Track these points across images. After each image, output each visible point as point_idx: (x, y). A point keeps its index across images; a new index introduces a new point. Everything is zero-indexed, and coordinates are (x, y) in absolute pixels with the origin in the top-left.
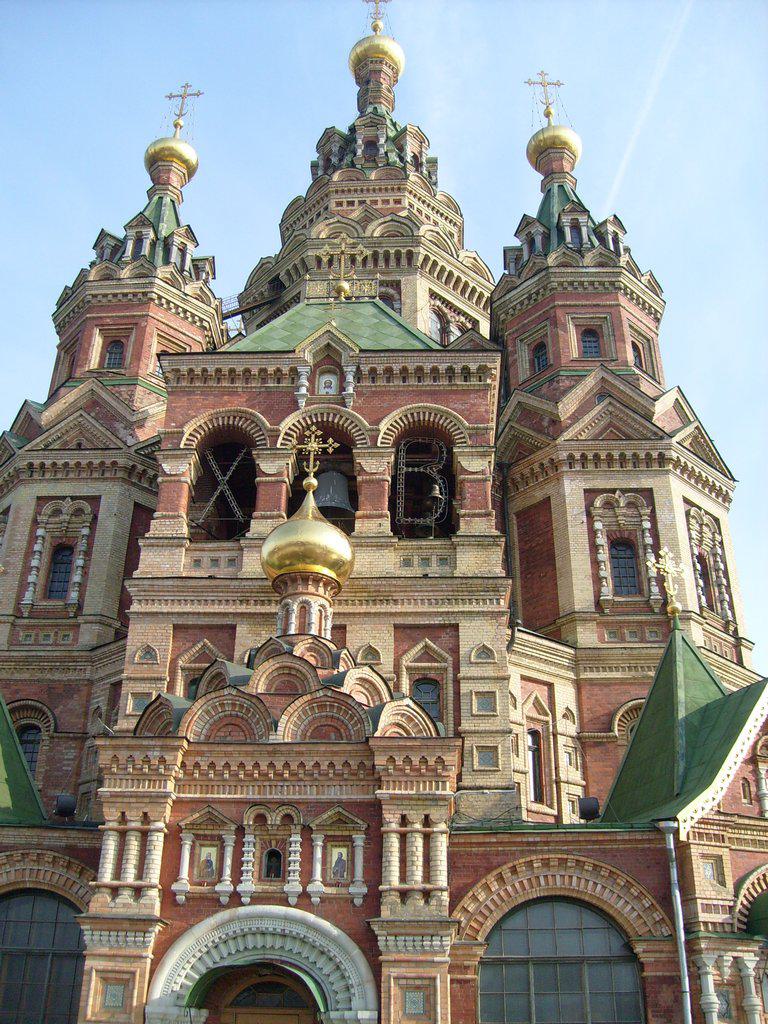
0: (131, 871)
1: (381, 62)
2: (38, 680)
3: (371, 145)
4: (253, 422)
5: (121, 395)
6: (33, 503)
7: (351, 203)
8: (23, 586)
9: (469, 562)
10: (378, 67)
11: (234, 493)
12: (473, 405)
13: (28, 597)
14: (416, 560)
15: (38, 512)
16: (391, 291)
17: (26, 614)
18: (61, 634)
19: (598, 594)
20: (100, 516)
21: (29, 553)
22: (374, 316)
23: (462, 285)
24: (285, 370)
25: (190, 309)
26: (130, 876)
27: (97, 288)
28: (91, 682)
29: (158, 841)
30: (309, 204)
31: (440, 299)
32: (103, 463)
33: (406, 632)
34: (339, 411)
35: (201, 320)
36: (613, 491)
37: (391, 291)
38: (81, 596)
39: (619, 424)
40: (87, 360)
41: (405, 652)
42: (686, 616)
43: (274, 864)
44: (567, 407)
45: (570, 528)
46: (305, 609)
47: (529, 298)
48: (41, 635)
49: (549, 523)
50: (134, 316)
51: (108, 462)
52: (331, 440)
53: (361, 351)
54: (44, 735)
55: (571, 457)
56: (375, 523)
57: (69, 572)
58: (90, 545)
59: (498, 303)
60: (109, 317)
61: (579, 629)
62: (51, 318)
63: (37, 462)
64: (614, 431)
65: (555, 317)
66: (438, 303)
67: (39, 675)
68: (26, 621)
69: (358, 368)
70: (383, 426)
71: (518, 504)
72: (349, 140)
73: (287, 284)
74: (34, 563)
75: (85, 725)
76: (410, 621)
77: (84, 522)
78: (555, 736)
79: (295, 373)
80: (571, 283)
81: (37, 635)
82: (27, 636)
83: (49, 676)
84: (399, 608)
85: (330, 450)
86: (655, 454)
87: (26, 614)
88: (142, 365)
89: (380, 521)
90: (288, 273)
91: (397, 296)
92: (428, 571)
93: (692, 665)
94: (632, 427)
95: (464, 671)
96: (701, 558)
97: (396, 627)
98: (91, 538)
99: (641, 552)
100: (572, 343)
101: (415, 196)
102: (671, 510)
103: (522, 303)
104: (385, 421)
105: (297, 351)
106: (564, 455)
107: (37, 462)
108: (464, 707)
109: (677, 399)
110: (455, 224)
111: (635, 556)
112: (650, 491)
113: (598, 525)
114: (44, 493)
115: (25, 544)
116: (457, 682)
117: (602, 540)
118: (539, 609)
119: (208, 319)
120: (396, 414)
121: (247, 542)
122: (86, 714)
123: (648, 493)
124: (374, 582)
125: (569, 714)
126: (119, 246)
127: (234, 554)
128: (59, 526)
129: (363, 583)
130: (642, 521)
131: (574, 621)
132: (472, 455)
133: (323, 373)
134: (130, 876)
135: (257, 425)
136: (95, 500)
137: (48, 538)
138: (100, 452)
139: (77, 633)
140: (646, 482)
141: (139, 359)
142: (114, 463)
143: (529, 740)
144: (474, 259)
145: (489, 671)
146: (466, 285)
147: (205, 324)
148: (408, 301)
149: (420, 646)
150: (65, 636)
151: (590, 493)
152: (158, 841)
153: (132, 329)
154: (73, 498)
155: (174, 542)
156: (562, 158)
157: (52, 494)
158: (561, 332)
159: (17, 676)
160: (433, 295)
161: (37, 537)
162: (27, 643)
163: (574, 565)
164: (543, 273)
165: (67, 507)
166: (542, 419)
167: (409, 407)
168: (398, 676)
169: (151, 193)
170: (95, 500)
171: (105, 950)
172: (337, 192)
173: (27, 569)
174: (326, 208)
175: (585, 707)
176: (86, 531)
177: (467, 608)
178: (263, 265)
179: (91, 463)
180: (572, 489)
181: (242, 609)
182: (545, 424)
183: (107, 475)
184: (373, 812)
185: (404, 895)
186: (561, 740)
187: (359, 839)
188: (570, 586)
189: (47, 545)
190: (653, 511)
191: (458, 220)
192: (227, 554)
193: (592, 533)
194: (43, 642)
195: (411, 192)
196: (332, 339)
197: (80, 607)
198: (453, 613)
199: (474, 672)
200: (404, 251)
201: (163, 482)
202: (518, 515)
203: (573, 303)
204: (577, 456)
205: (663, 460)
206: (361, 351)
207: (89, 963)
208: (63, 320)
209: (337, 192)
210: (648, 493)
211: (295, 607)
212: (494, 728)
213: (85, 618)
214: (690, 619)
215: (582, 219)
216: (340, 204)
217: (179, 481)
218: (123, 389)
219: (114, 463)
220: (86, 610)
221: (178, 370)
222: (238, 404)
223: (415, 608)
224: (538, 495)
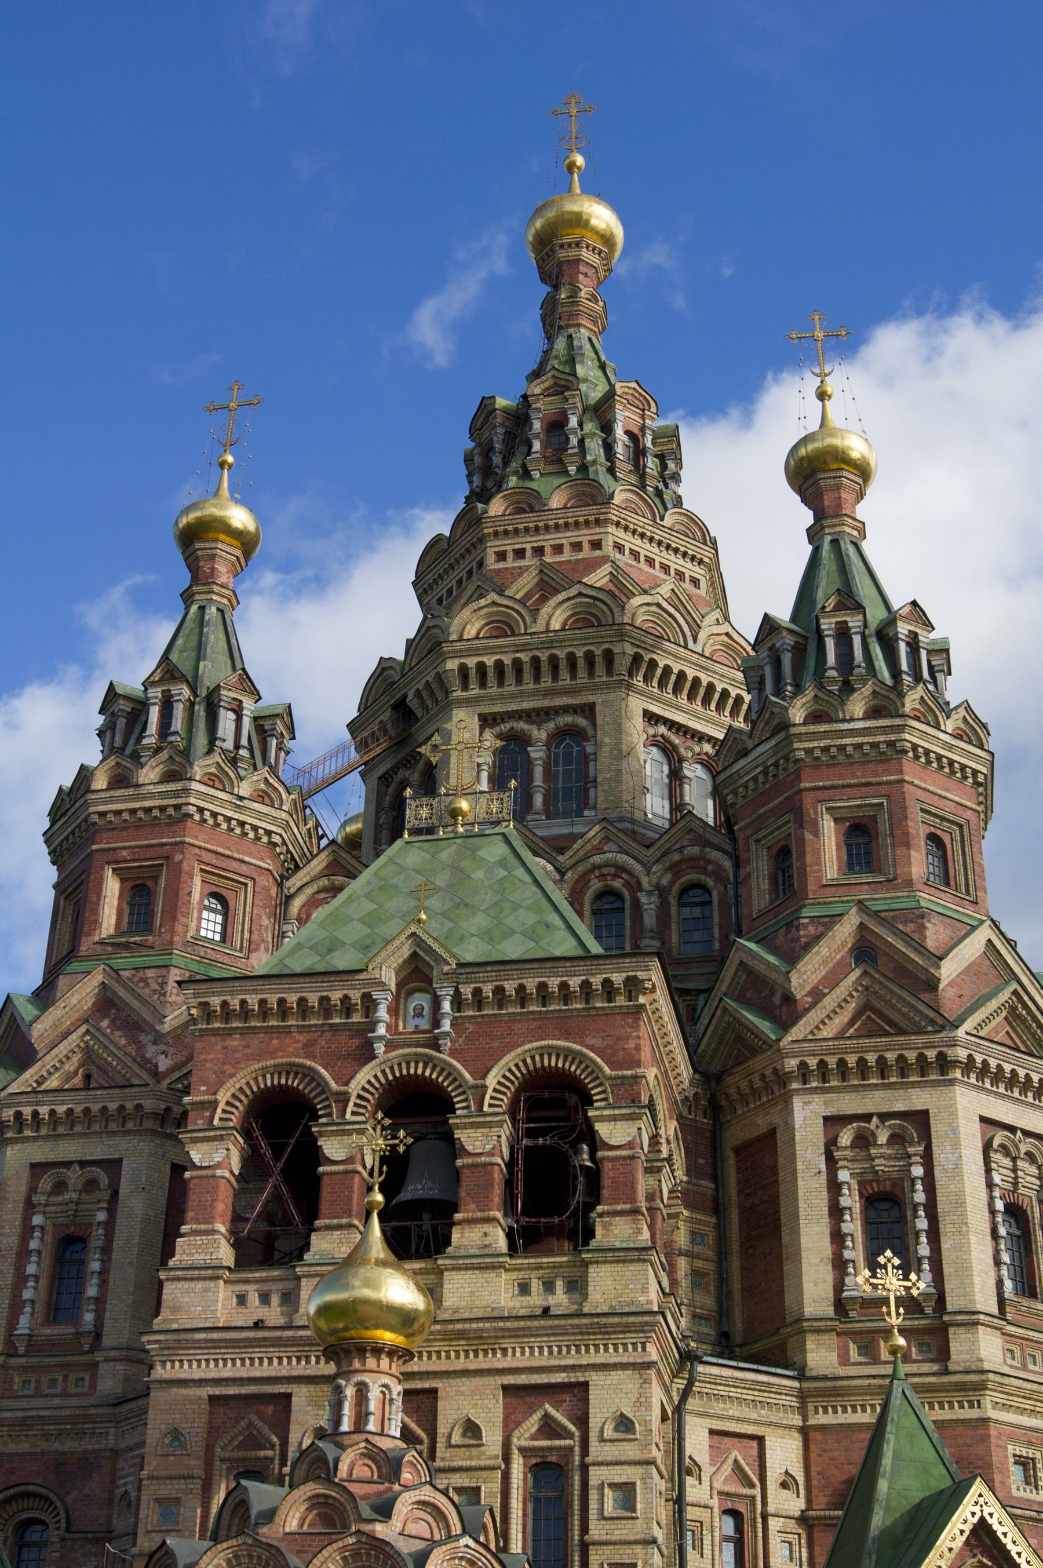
1: (578, 245)
2: (42, 1453)
3: (557, 426)
4: (313, 1079)
5: (147, 985)
6: (25, 1174)
7: (520, 554)
8: (16, 1306)
9: (605, 1286)
10: (572, 253)
12: (619, 1039)
13: (24, 1321)
14: (536, 1285)
15: (33, 1189)
16: (582, 722)
17: (22, 1350)
18: (72, 1377)
19: (839, 1287)
20: (122, 1191)
21: (23, 1254)
22: (502, 863)
23: (702, 691)
24: (356, 996)
25: (249, 820)
27: (105, 802)
28: (116, 1453)
30: (458, 550)
31: (665, 724)
32: (122, 1108)
33: (519, 1395)
34: (431, 1058)
35: (269, 833)
36: (867, 1117)
37: (582, 722)
39: (880, 1005)
40: (96, 923)
41: (518, 1424)
42: (971, 1321)
44: (804, 977)
45: (800, 1183)
46: (362, 1390)
47: (765, 772)
48: (45, 1379)
49: (774, 1169)
50: (163, 845)
51: (130, 1106)
52: (402, 1134)
53: (460, 965)
54: (54, 1535)
55: (803, 1065)
56: (480, 1233)
57: (81, 1279)
58: (109, 1237)
60: (124, 848)
61: (810, 1345)
62: (42, 839)
64: (873, 1018)
65: (801, 808)
66: (662, 729)
67: (43, 1445)
68: (21, 1361)
69: (457, 989)
70: (491, 1081)
71: (737, 1133)
72: (520, 417)
73: (419, 713)
74: (31, 1269)
75: (109, 1518)
76: (523, 1379)
77: (99, 1202)
78: (765, 1517)
79: (369, 1004)
80: (826, 749)
81: (38, 1381)
82: (25, 1382)
83: (57, 1446)
84: (508, 1362)
85: (401, 1149)
86: (931, 1054)
87: (22, 1350)
88: (179, 929)
89: (487, 1228)
90: (418, 694)
91: (590, 731)
92: (552, 1300)
93: (911, 1437)
94: (899, 1011)
95: (596, 1450)
96: (1015, 1212)
97: (506, 1389)
98: (109, 1226)
99: (909, 1213)
100: (827, 847)
101: (626, 528)
102: (956, 1145)
103: (755, 779)
104: (494, 1071)
105: (370, 968)
106: (792, 1063)
108: (593, 1506)
109: (989, 941)
110: (701, 562)
111: (902, 1220)
112: (925, 1113)
113: (843, 1175)
114: (39, 1158)
115: (15, 1240)
116: (584, 1468)
117: (850, 1200)
118: (746, 1315)
119: (279, 831)
120: (509, 1060)
121: (305, 1269)
122: (110, 1500)
123: (921, 1119)
124: (474, 1325)
125: (790, 1481)
126: (139, 708)
127: (289, 1285)
128: (65, 1208)
129: (459, 1326)
130: (910, 1165)
131: (803, 1332)
132: (614, 1119)
133: (411, 993)
135: (319, 1085)
136: (113, 1166)
137: (49, 1228)
138: (117, 1091)
139: (94, 1376)
140: (918, 1099)
141: (174, 919)
142: (139, 1107)
143: (728, 1526)
144: (727, 634)
145: (630, 1451)
146: (711, 687)
147: (276, 839)
148: (607, 740)
149: (539, 1414)
150: (78, 1380)
151: (833, 1122)
153: (162, 865)
154: (83, 1164)
155: (210, 1272)
156: (838, 487)
157: (52, 1157)
158: (808, 836)
160: (650, 718)
161: (33, 1228)
162: (25, 1392)
163: (805, 1242)
164: (782, 735)
165: (74, 1177)
166: (773, 993)
167: (527, 1047)
168: (507, 1458)
170: (113, 1166)
173: (21, 1280)
174: (481, 564)
175: (814, 1470)
177: (601, 1358)
178: (385, 666)
179: (105, 1109)
180: (807, 1115)
181: (300, 1369)
182: (777, 1000)
183: (130, 1125)
186: (774, 1524)
188: (799, 1276)
189: (48, 1238)
190: (928, 1148)
191: (706, 554)
192: (280, 1286)
193: (834, 1187)
194: (47, 1391)
195: (618, 524)
196: (418, 946)
197: (98, 1335)
198: (580, 1366)
199: (610, 1452)
200: (598, 651)
201: (192, 1178)
202: (737, 1151)
203: (828, 783)
204: (812, 1062)
205: (944, 1063)
206: (460, 965)
208: (60, 844)
209: (496, 534)
210: (921, 1119)
211: (350, 1392)
212: (632, 1538)
213: (105, 1353)
214: (976, 1323)
215: (854, 622)
217: (214, 1176)
218: (150, 973)
219: (139, 1107)
220: (107, 1341)
221: (207, 1004)
222: (291, 1052)
223: (533, 1358)
224: (761, 1124)
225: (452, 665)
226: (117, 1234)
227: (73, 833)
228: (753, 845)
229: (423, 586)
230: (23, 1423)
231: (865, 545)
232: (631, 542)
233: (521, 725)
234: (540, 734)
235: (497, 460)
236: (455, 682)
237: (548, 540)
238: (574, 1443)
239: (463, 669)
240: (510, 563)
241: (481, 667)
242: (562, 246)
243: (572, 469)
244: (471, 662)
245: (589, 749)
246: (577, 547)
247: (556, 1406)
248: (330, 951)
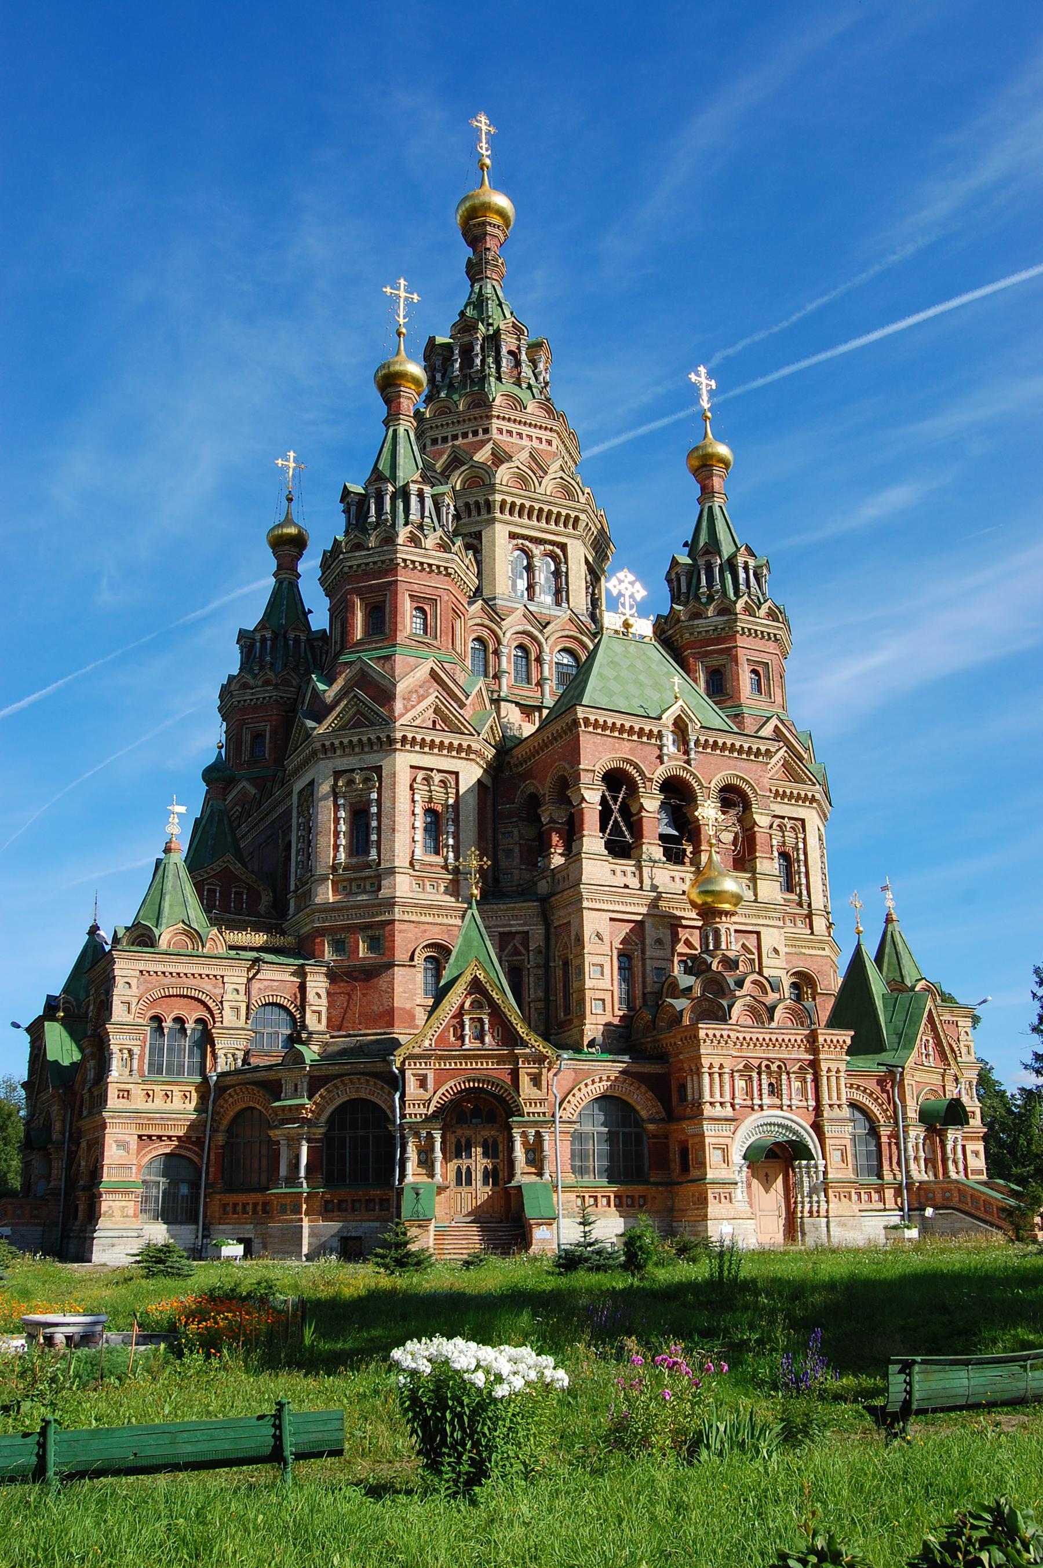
0: (715, 1095)
11: (624, 820)
16: (558, 551)
22: (660, 661)
26: (717, 1097)
29: (726, 1077)
43: (775, 1090)
53: (702, 727)
63: (410, 736)
83: (445, 921)
107: (410, 736)
132: (762, 814)
134: (717, 1097)
140: (801, 812)
152: (726, 1077)
159: (423, 919)
165: (437, 777)
169: (387, 423)
171: (713, 1133)
172: (498, 417)
184: (814, 1064)
185: (831, 1106)
187: (809, 1077)
207: (707, 1140)
208: (359, 566)
216: (500, 431)
225: (498, 497)
226: (461, 813)
227: (375, 563)
230: (430, 907)
233: (527, 543)
237: (526, 430)
238: (756, 957)
239: (503, 502)
241: (513, 504)
242: (490, 224)
243: (524, 386)
244: (509, 499)
245: (564, 569)
247: (747, 939)
248: (611, 696)
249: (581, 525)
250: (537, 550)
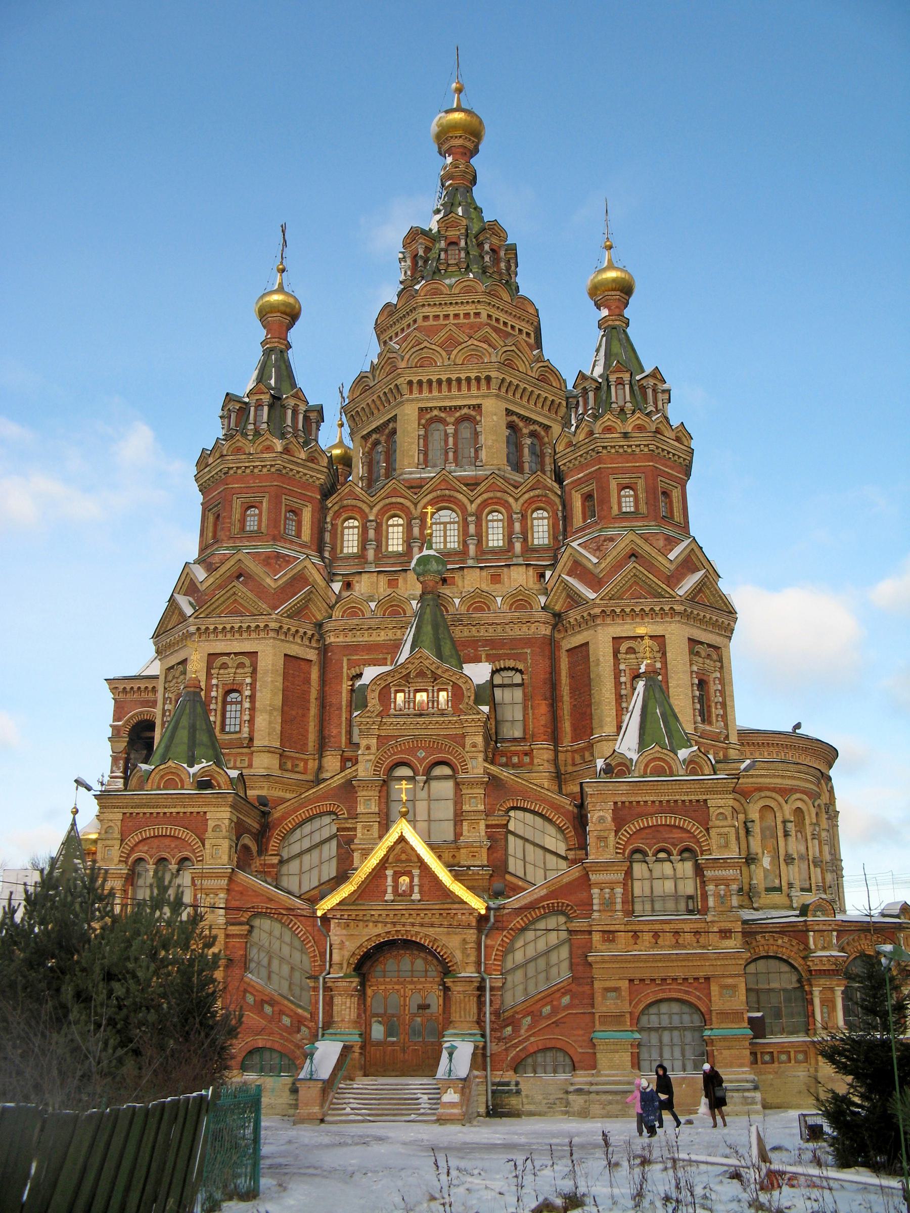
16: (473, 413)
37: (473, 413)
38: (251, 732)
59: (559, 455)
66: (515, 418)
91: (478, 418)
96: (702, 684)
98: (253, 686)
137: (221, 686)
151: (617, 640)
174: (415, 321)
176: (248, 680)
189: (220, 690)
190: (664, 654)
197: (251, 739)
215: (626, 377)
216: (426, 318)
220: (256, 743)
228: (573, 492)
229: (380, 329)
231: (628, 330)
232: (496, 314)
234: (451, 420)
235: (420, 263)
236: (405, 389)
237: (451, 311)
240: (431, 322)
246: (467, 315)
249: (494, 384)
250: (451, 420)
